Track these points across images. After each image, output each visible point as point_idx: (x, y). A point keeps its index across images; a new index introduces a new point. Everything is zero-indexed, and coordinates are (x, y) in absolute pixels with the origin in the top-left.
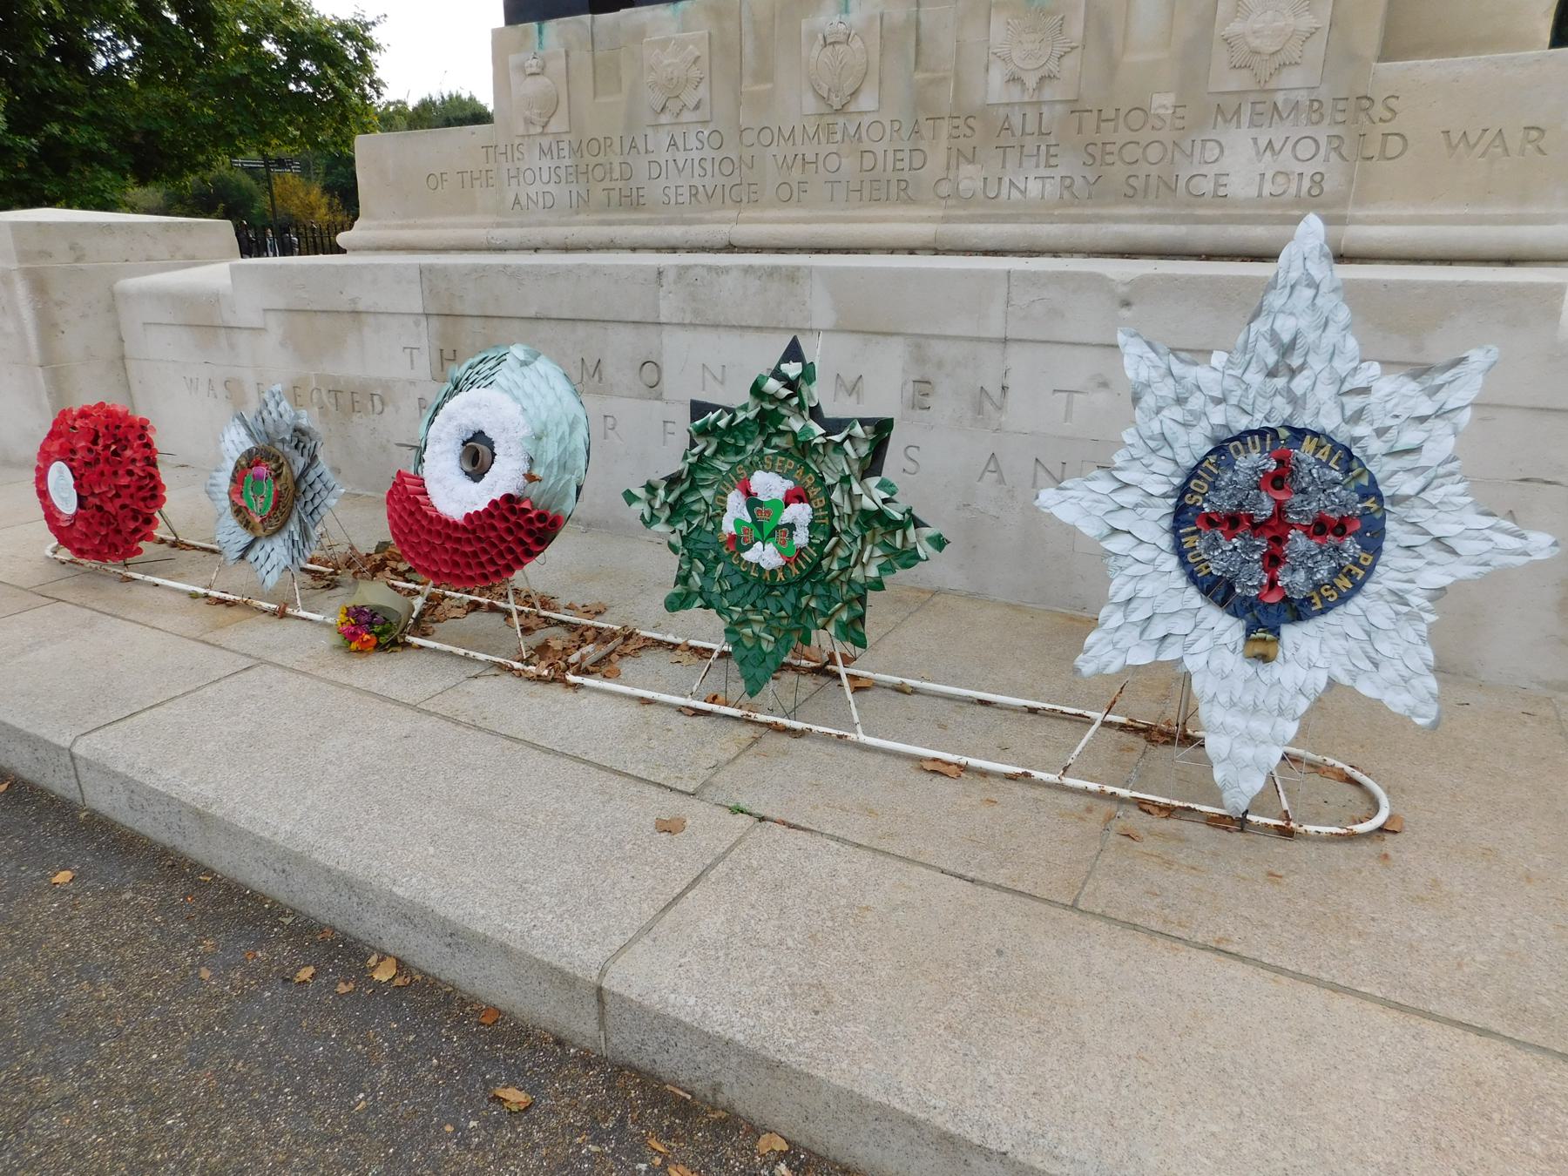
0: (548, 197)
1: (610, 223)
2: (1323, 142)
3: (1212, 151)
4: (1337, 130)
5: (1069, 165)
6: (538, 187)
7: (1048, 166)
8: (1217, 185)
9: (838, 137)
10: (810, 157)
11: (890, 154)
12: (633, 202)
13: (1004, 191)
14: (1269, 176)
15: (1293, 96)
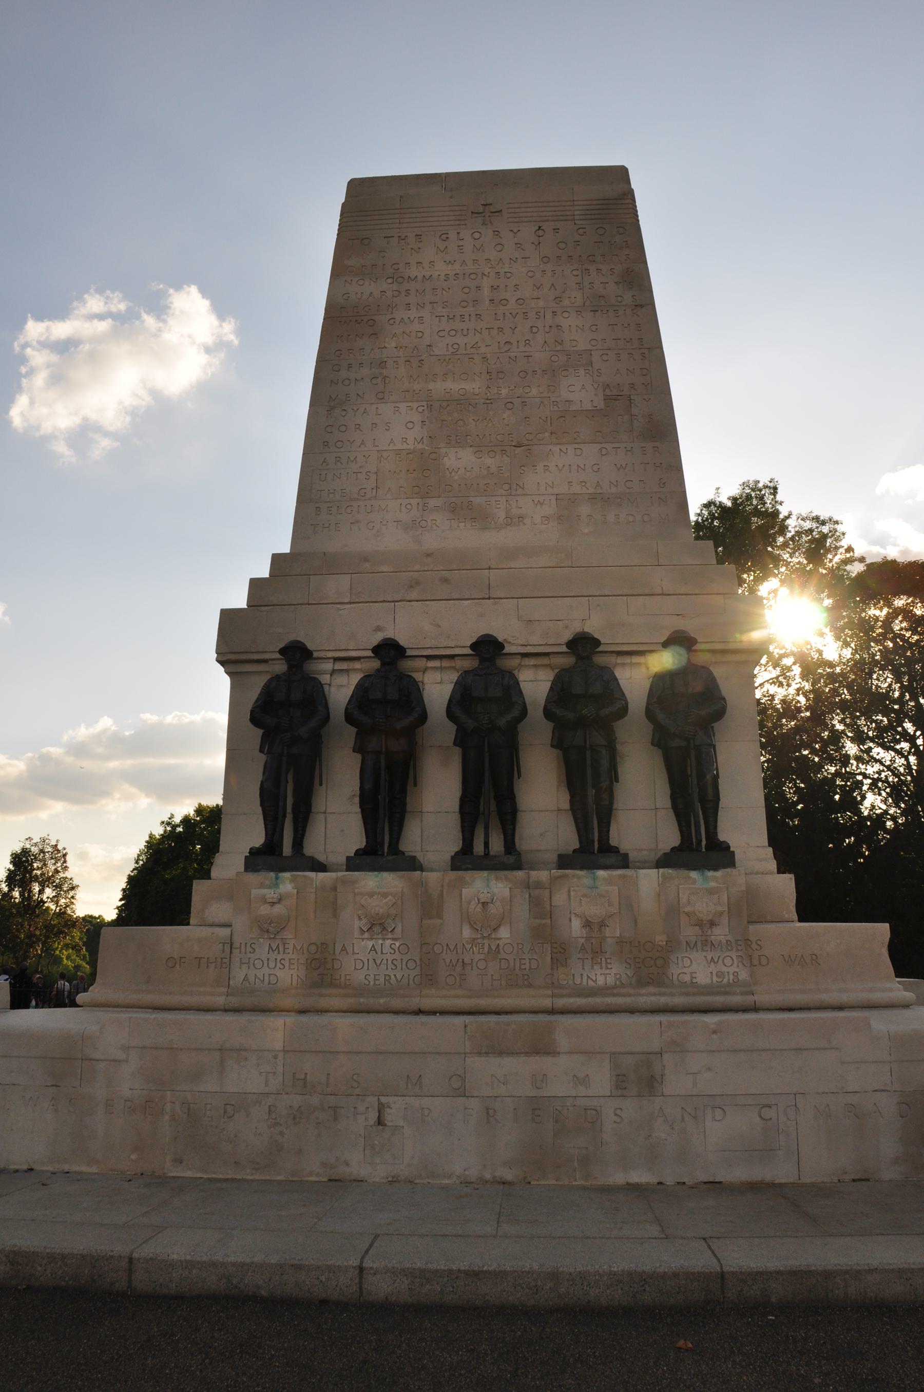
0: (272, 977)
2: (734, 958)
3: (687, 962)
4: (739, 954)
7: (607, 968)
8: (692, 978)
9: (486, 950)
10: (467, 961)
11: (518, 961)
13: (585, 981)
14: (714, 973)
15: (718, 938)
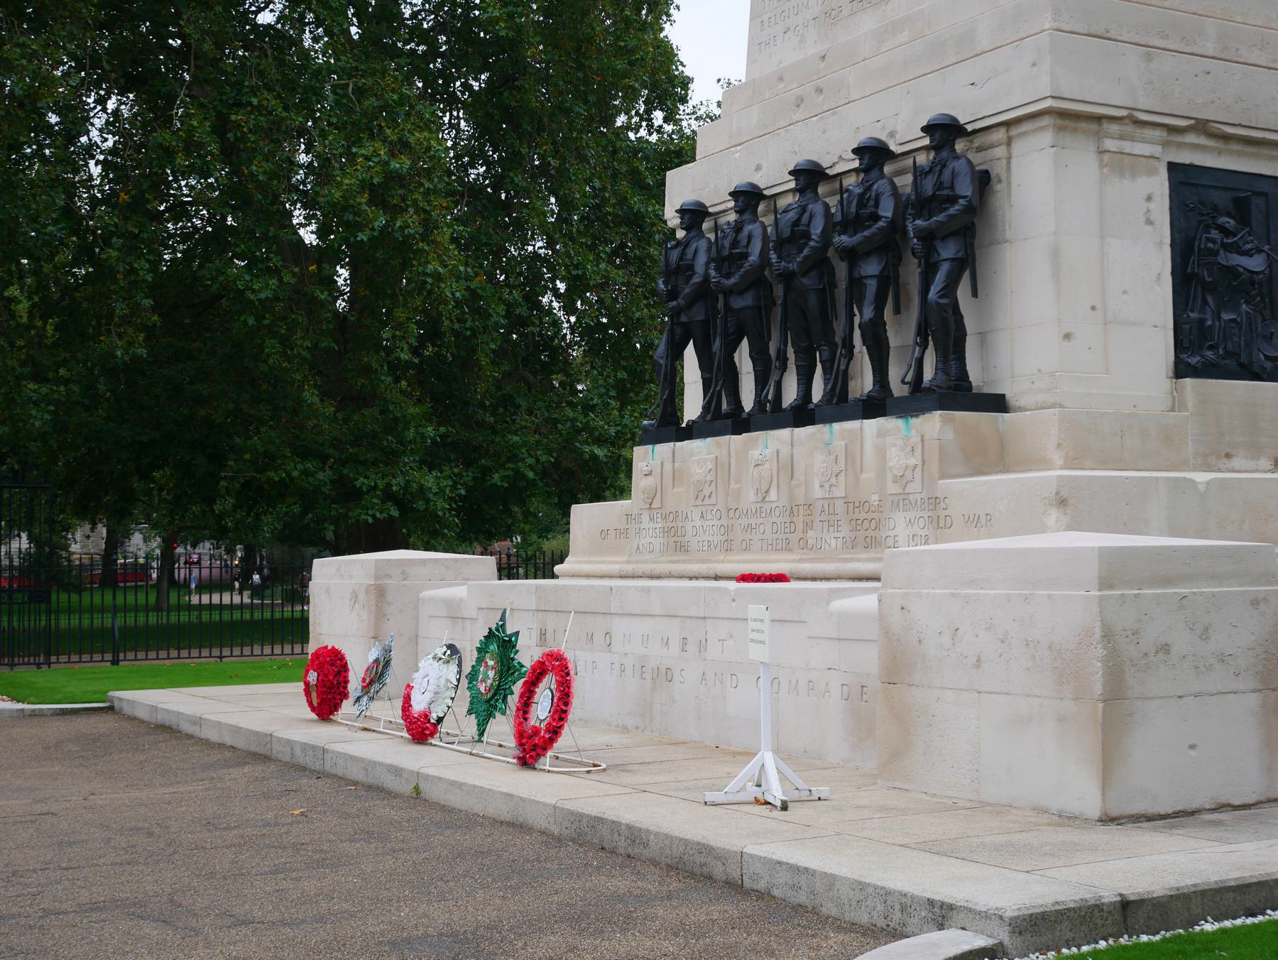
1: (674, 562)
5: (845, 531)
6: (648, 540)
12: (682, 548)
